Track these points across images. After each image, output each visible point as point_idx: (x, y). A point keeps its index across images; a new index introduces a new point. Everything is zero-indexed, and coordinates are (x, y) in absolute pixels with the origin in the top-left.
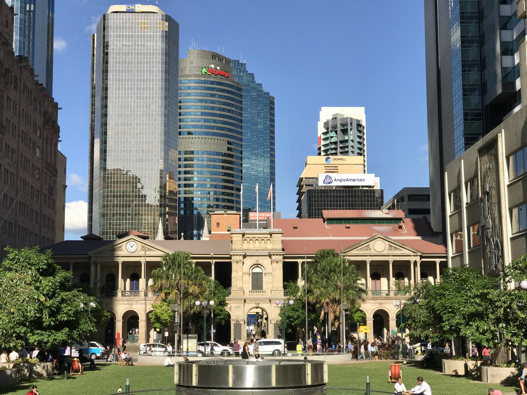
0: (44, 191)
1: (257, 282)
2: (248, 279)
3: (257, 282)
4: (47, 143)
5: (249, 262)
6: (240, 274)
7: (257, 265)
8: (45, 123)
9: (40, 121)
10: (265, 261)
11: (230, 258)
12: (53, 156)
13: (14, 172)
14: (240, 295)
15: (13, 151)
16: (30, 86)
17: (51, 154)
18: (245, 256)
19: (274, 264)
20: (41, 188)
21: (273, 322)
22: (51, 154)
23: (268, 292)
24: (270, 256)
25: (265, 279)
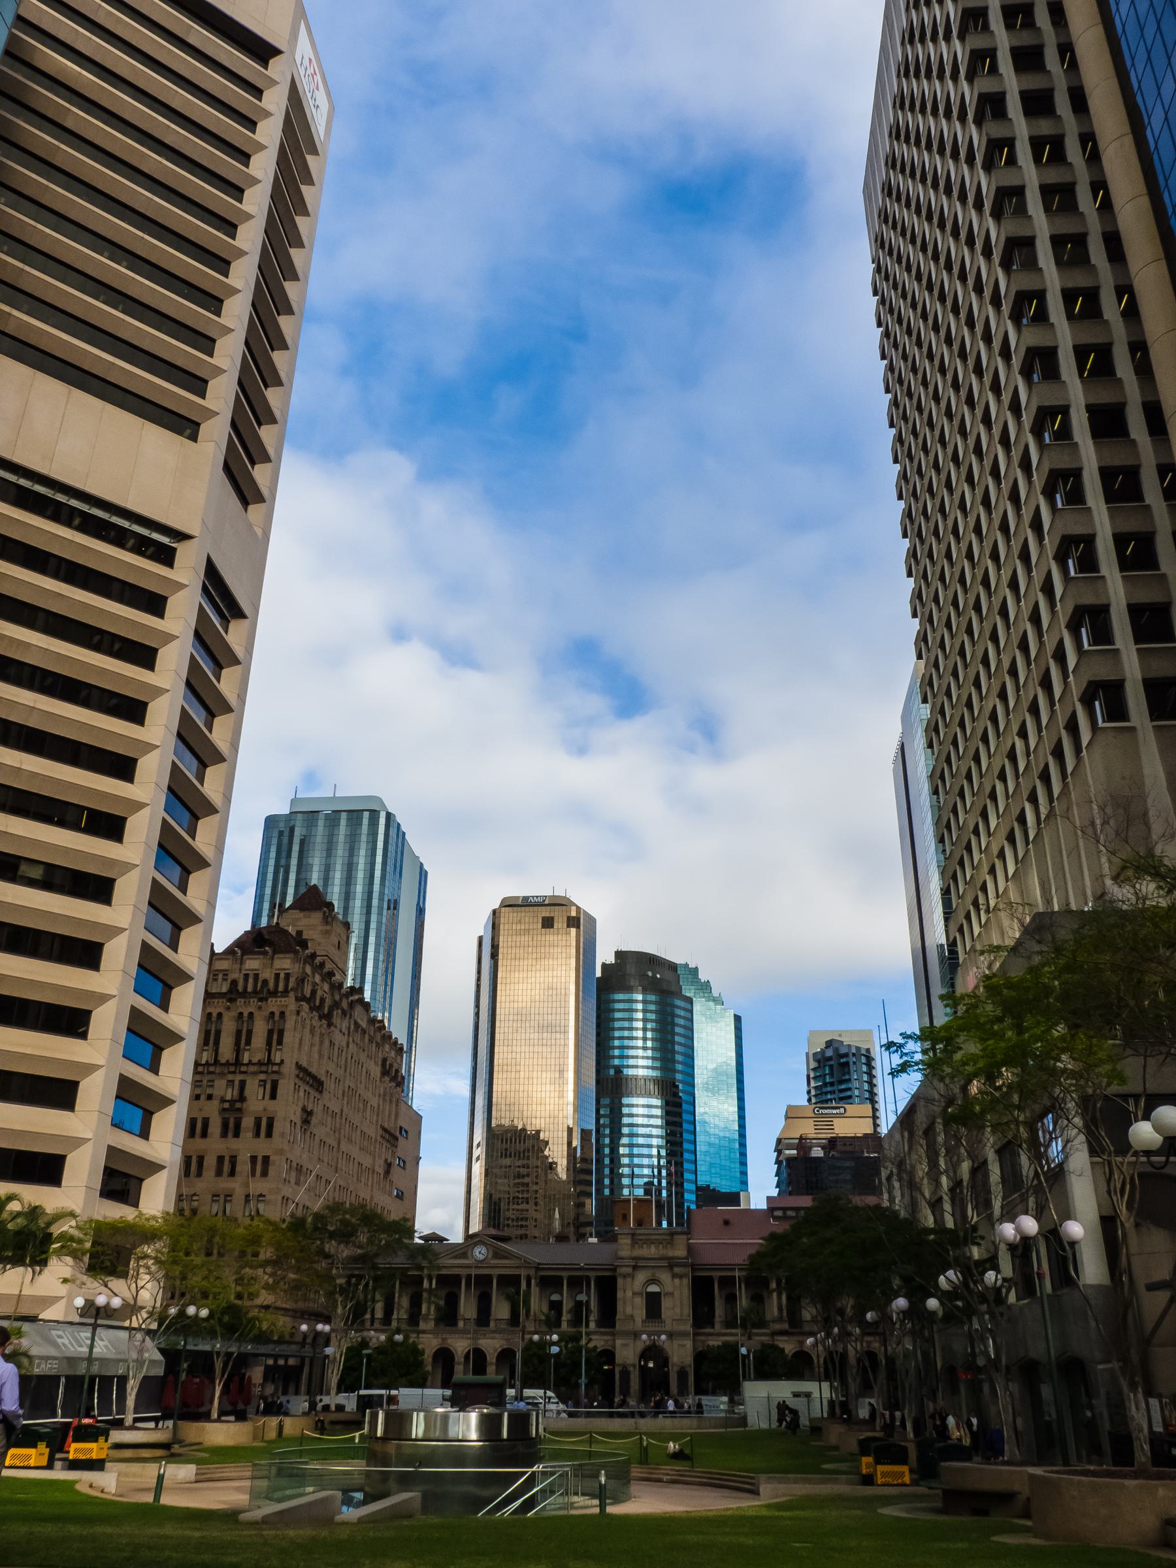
0: (377, 1169)
1: (653, 1304)
2: (640, 1302)
3: (653, 1304)
4: (384, 1100)
5: (641, 1277)
6: (629, 1294)
7: (653, 1281)
8: (385, 1072)
9: (376, 1071)
10: (665, 1277)
11: (614, 1270)
12: (393, 1117)
13: (335, 1144)
14: (629, 1327)
15: (334, 1115)
16: (364, 1024)
17: (390, 1115)
18: (635, 1268)
19: (677, 1281)
20: (374, 1165)
21: (676, 1369)
22: (390, 1115)
23: (668, 1322)
24: (671, 1267)
25: (666, 1303)
